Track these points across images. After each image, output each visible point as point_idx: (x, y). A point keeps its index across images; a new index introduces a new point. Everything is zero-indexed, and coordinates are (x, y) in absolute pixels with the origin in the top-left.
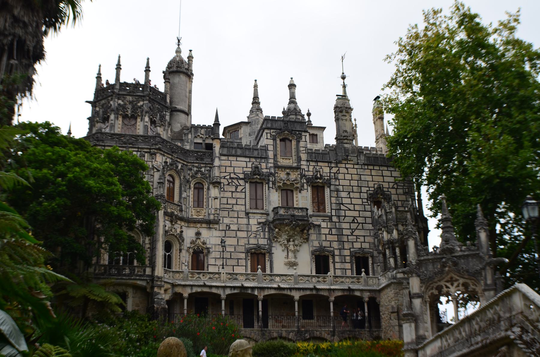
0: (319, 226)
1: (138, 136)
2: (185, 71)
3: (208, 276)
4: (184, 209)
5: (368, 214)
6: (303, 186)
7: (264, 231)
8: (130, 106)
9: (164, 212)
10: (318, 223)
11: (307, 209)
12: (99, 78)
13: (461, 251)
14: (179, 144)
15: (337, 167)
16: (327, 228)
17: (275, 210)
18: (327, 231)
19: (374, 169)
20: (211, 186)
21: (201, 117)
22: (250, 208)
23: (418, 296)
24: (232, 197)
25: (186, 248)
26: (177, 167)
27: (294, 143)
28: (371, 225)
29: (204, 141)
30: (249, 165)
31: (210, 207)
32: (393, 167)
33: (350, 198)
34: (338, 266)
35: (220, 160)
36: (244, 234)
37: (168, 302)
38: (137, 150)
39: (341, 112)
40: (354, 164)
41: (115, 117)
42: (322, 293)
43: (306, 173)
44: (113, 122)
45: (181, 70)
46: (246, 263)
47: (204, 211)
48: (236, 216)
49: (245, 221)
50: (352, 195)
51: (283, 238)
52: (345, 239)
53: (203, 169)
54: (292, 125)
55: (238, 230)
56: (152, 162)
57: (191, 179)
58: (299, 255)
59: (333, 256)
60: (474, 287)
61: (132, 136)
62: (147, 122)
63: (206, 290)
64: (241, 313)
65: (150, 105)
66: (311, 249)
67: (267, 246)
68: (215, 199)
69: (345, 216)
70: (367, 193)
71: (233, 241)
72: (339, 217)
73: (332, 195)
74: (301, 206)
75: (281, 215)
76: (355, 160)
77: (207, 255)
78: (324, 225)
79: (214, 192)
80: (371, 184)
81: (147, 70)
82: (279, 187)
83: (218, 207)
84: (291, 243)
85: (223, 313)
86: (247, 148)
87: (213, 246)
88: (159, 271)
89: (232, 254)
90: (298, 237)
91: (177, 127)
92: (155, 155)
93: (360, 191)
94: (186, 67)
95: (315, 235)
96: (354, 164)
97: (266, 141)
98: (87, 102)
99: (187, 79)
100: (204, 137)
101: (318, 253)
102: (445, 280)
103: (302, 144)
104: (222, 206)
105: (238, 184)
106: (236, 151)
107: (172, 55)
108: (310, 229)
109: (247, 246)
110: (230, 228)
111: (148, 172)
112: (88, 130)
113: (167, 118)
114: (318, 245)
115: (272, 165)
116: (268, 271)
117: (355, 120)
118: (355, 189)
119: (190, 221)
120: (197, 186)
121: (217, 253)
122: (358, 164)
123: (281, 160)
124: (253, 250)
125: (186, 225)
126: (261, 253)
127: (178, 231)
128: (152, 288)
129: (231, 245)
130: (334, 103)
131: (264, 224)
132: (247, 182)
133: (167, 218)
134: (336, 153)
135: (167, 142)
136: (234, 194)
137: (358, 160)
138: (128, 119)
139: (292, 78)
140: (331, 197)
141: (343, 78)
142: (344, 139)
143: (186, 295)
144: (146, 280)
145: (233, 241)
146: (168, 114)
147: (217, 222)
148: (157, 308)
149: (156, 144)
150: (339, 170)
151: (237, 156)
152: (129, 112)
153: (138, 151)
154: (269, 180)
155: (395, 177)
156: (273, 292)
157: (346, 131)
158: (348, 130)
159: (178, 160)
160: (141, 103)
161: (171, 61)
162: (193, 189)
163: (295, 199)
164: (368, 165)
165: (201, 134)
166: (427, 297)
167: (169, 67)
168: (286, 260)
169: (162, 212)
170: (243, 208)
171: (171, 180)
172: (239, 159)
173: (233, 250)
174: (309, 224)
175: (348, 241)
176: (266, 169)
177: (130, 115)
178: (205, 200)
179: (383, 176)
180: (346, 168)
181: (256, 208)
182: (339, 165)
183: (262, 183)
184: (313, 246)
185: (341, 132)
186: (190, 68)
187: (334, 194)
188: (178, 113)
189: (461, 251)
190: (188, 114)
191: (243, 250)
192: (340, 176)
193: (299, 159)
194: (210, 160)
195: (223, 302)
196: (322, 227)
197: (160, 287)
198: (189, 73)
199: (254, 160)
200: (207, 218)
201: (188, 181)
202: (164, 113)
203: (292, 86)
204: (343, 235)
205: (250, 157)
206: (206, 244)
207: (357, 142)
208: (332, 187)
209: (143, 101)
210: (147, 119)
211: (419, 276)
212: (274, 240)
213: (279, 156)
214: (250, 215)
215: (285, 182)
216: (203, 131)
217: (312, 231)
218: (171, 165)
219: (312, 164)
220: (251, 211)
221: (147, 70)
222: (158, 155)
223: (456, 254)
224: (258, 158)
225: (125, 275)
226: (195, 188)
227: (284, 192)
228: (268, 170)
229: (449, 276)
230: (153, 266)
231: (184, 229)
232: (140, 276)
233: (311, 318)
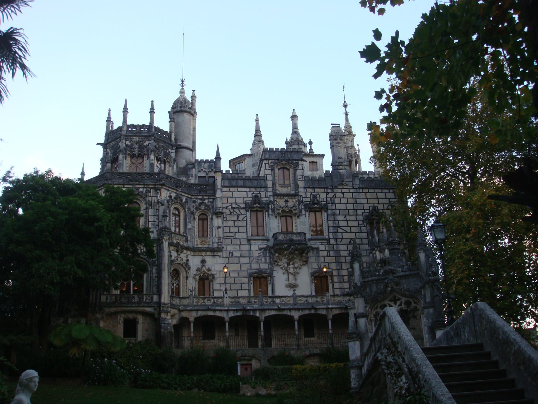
0: (318, 249)
1: (143, 174)
2: (189, 110)
3: (212, 301)
4: (189, 239)
5: (365, 235)
6: (301, 212)
7: (265, 256)
8: (137, 146)
9: (169, 243)
10: (316, 246)
11: (305, 234)
12: (109, 120)
13: (402, 271)
14: (185, 179)
15: (333, 192)
16: (325, 250)
17: (275, 235)
18: (325, 253)
19: (368, 192)
20: (214, 217)
21: (204, 152)
22: (252, 236)
23: (363, 316)
24: (234, 226)
25: (192, 275)
26: (181, 200)
27: (291, 171)
28: (367, 246)
29: (207, 174)
30: (250, 194)
31: (214, 236)
32: (387, 189)
33: (346, 220)
34: (336, 285)
35: (222, 191)
36: (246, 260)
37: (175, 326)
38: (143, 186)
39: (336, 140)
40: (349, 189)
41: (123, 157)
42: (320, 312)
43: (304, 200)
44: (121, 162)
45: (185, 109)
46: (249, 287)
48: (239, 243)
49: (247, 248)
50: (348, 218)
51: (284, 262)
52: (343, 260)
53: (206, 201)
54: (293, 154)
55: (241, 257)
56: (157, 197)
57: (195, 211)
58: (299, 277)
59: (332, 276)
60: (415, 305)
61: (139, 174)
62: (152, 160)
63: (210, 313)
64: (246, 334)
65: (155, 144)
66: (310, 271)
67: (268, 271)
68: (218, 228)
69: (342, 238)
70: (362, 215)
71: (237, 267)
72: (336, 239)
73: (330, 219)
74: (299, 231)
75: (280, 240)
76: (350, 184)
77: (212, 281)
78: (322, 247)
79: (217, 222)
80: (366, 207)
81: (152, 111)
82: (279, 214)
83: (221, 236)
84: (291, 266)
85: (227, 334)
86: (248, 179)
87: (218, 273)
88: (165, 298)
89: (236, 279)
90: (297, 260)
91: (182, 163)
92: (160, 190)
93: (355, 214)
94: (190, 106)
95: (314, 258)
96: (349, 189)
97: (265, 171)
98: (98, 144)
99: (191, 117)
100: (207, 171)
101: (317, 274)
102: (388, 299)
103: (299, 172)
104: (225, 235)
105: (239, 213)
106: (237, 183)
107: (176, 96)
108: (308, 252)
109: (249, 271)
110: (233, 255)
111: (154, 207)
112: (100, 170)
113: (173, 155)
114: (317, 267)
115: (271, 194)
116: (270, 294)
117: (358, 145)
118: (351, 212)
119: (195, 250)
120: (201, 217)
121: (222, 279)
122: (353, 188)
123: (280, 189)
124: (255, 275)
125: (192, 253)
126: (263, 277)
127: (185, 259)
128: (159, 314)
129: (234, 271)
130: (330, 131)
131: (265, 249)
132: (248, 211)
133: (172, 248)
134: (332, 179)
135: (171, 178)
136: (236, 223)
137: (353, 184)
138: (135, 158)
139: (294, 110)
140: (328, 221)
141: (345, 106)
142: (339, 166)
143: (192, 319)
144: (154, 307)
145: (237, 267)
146: (173, 151)
147: (219, 250)
148: (164, 333)
149: (158, 180)
150: (335, 195)
151: (238, 187)
152: (136, 152)
153: (144, 188)
154: (268, 208)
155: (389, 199)
156: (273, 313)
157: (340, 158)
158: (343, 157)
159: (183, 194)
160: (147, 143)
161: (175, 102)
162: (197, 220)
163: (294, 225)
164: (363, 188)
166: (372, 316)
167: (173, 108)
168: (287, 283)
169: (167, 243)
170: (244, 235)
171: (177, 212)
172: (240, 189)
173: (236, 275)
174: (308, 247)
175: (346, 262)
176: (266, 197)
177: (137, 155)
178: (209, 230)
179: (377, 198)
180: (341, 192)
181: (258, 235)
182: (335, 190)
183: (262, 211)
184: (312, 268)
185: (336, 159)
186: (193, 107)
187: (331, 218)
188: (184, 150)
189: (402, 271)
190: (193, 150)
191: (246, 274)
192: (337, 201)
193: (297, 187)
194: (212, 192)
195: (227, 324)
196: (320, 249)
197: (167, 312)
198: (193, 112)
199: (254, 190)
201: (193, 213)
202: (170, 150)
203: (294, 117)
204: (340, 256)
205: (250, 187)
206: (211, 270)
207: (360, 167)
208: (329, 212)
209: (149, 141)
210: (152, 157)
211: (363, 297)
213: (277, 185)
214: (251, 242)
215: (284, 209)
216: (206, 165)
217: (310, 254)
218: (175, 198)
219: (310, 190)
220: (253, 238)
221: (152, 111)
222: (163, 190)
223: (398, 275)
224: (258, 187)
225: (134, 303)
226: (199, 219)
227: (284, 218)
228: (268, 199)
229: (392, 296)
230: (159, 293)
231: (190, 258)
232: (149, 303)
233: (313, 336)
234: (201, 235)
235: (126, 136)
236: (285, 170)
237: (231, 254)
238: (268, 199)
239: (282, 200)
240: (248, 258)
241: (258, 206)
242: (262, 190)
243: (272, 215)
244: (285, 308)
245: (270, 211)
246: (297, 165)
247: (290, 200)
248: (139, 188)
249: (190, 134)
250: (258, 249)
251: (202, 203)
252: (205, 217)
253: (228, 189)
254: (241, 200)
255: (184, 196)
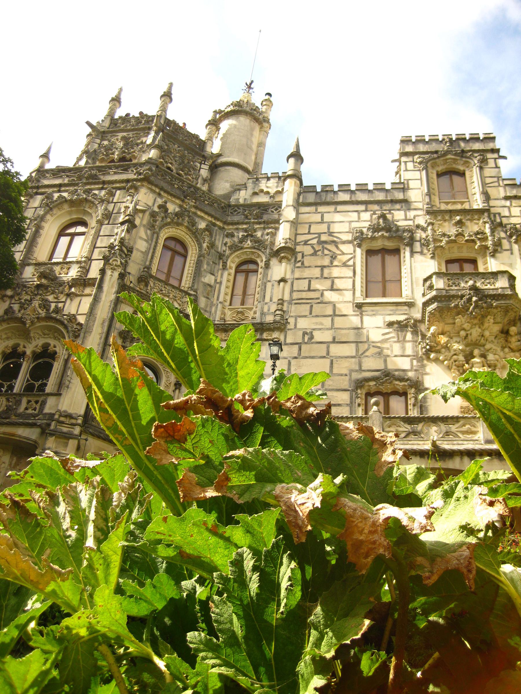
6: (498, 244)
20: (274, 262)
26: (193, 224)
31: (267, 299)
36: (349, 350)
38: (101, 186)
47: (254, 309)
48: (330, 312)
53: (259, 234)
55: (334, 341)
79: (279, 269)
83: (287, 297)
92: (136, 189)
99: (257, 127)
100: (272, 191)
104: (295, 295)
109: (356, 376)
110: (312, 337)
111: (115, 220)
124: (372, 383)
136: (326, 271)
146: (207, 167)
153: (102, 188)
159: (199, 213)
162: (233, 271)
165: (267, 187)
169: (116, 274)
170: (348, 296)
171: (179, 248)
172: (340, 208)
176: (406, 219)
178: (258, 289)
181: (384, 296)
191: (345, 383)
199: (376, 207)
200: (259, 321)
212: (428, 358)
218: (177, 214)
220: (369, 300)
222: (143, 191)
226: (237, 271)
234: (237, 300)
235: (104, 132)
236: (455, 178)
237: (306, 338)
238: (411, 223)
239: (446, 224)
240: (353, 345)
241: (386, 234)
242: (398, 206)
243: (421, 253)
244: (455, 447)
245: (417, 247)
246: (484, 161)
247: (468, 223)
248: (92, 190)
249: (251, 148)
250: (381, 324)
251: (247, 236)
252: (252, 267)
253: (312, 209)
254: (345, 227)
255: (202, 218)
